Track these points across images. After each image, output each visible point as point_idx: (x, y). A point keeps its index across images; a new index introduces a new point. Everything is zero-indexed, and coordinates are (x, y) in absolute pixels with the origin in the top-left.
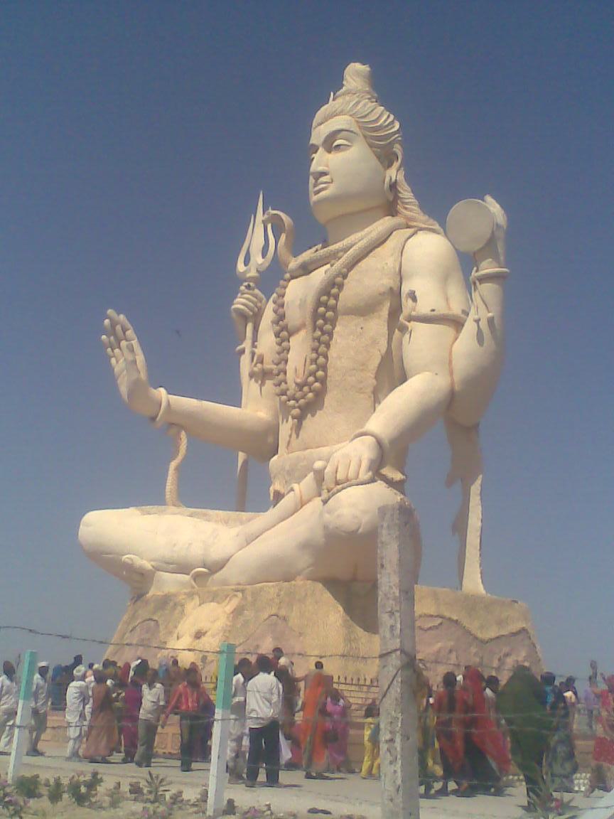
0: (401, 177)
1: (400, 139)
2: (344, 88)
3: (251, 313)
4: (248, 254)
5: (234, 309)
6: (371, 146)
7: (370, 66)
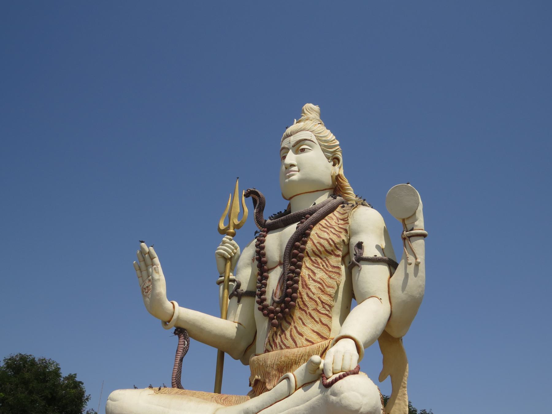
0: (342, 172)
1: (340, 149)
2: (303, 117)
3: (230, 256)
4: (229, 216)
5: (217, 253)
6: (324, 151)
7: (319, 107)
